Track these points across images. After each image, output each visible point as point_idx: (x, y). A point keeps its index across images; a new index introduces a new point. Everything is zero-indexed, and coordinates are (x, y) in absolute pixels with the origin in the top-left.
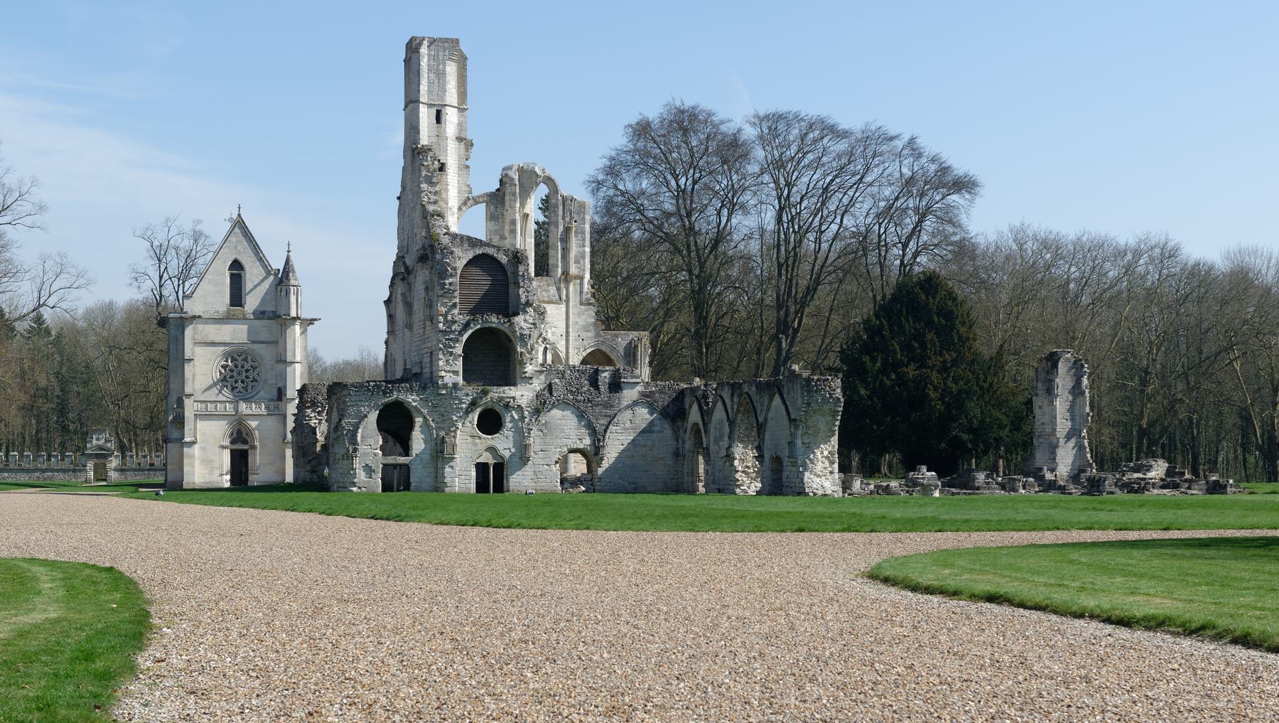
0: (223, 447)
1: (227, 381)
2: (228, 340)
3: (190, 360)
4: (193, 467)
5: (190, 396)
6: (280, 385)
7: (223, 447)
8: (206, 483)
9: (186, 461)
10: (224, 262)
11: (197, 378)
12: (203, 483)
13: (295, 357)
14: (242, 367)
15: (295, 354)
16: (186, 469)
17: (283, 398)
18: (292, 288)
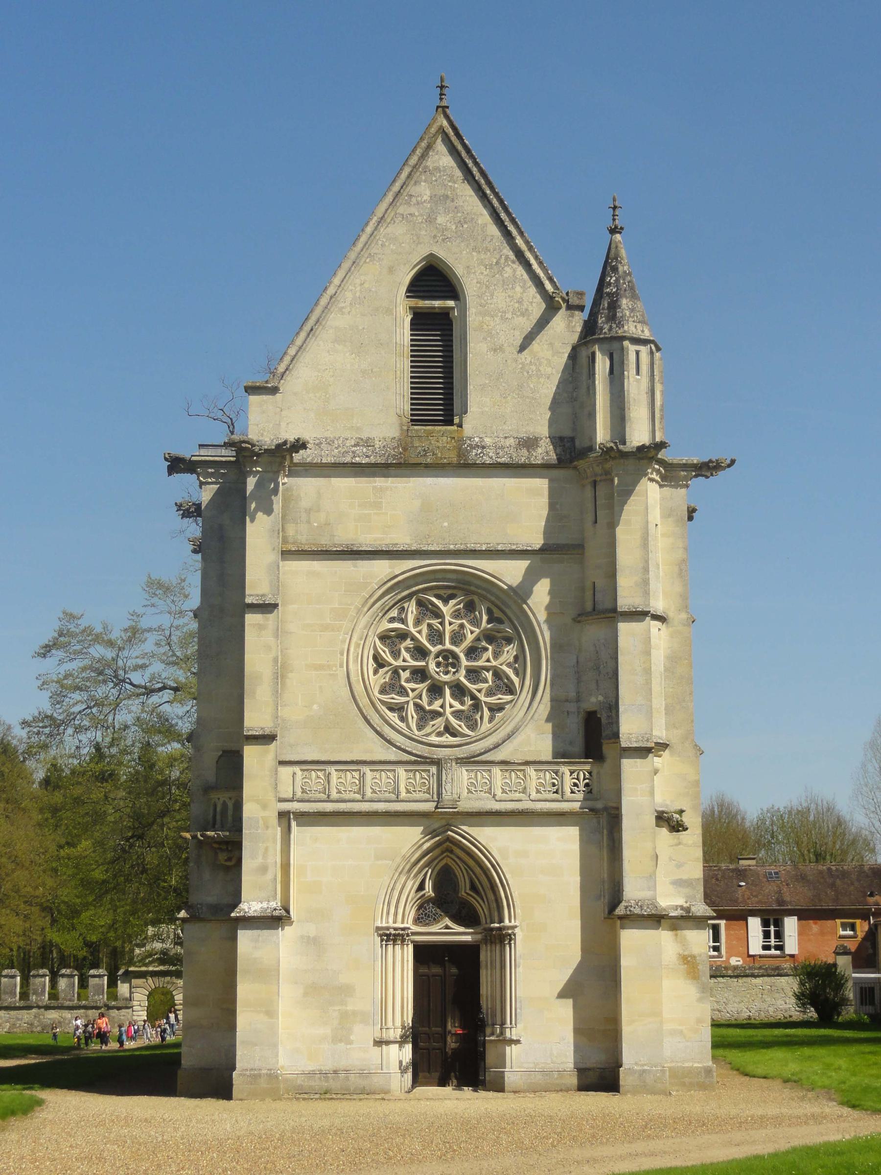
0: (391, 937)
1: (403, 692)
2: (403, 540)
3: (267, 608)
4: (271, 1013)
5: (267, 739)
6: (594, 701)
7: (391, 937)
8: (324, 1074)
9: (244, 990)
10: (391, 270)
11: (293, 679)
12: (312, 1074)
13: (646, 593)
14: (457, 638)
15: (646, 582)
16: (244, 1020)
17: (607, 749)
18: (632, 349)
